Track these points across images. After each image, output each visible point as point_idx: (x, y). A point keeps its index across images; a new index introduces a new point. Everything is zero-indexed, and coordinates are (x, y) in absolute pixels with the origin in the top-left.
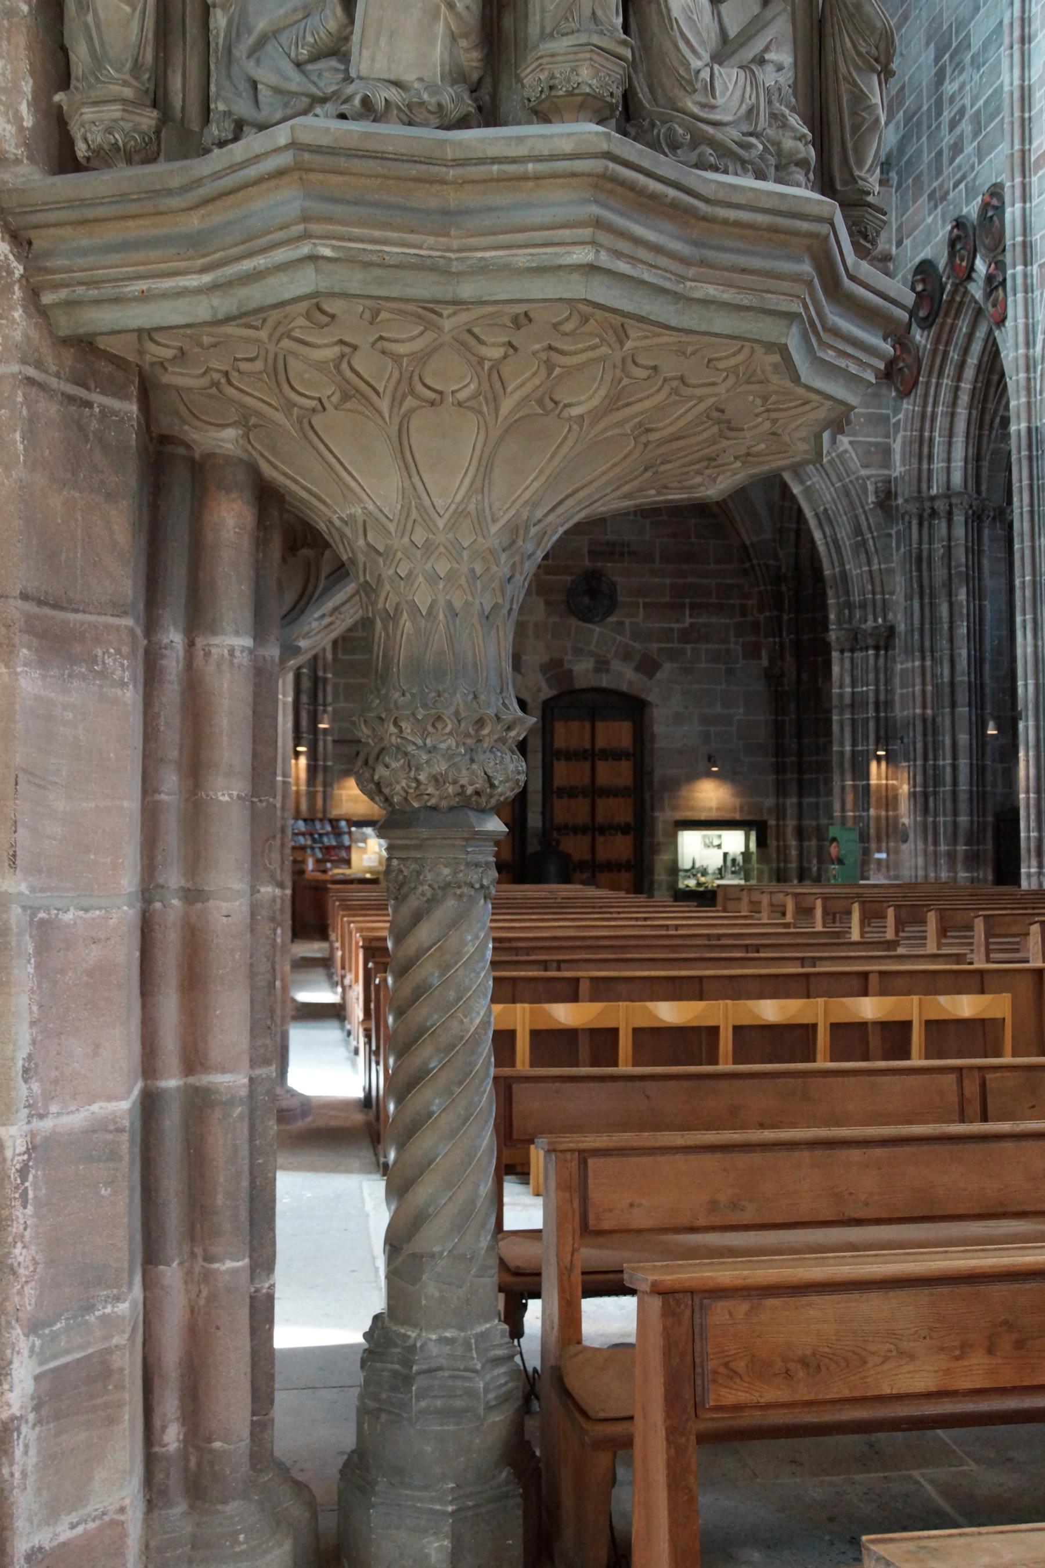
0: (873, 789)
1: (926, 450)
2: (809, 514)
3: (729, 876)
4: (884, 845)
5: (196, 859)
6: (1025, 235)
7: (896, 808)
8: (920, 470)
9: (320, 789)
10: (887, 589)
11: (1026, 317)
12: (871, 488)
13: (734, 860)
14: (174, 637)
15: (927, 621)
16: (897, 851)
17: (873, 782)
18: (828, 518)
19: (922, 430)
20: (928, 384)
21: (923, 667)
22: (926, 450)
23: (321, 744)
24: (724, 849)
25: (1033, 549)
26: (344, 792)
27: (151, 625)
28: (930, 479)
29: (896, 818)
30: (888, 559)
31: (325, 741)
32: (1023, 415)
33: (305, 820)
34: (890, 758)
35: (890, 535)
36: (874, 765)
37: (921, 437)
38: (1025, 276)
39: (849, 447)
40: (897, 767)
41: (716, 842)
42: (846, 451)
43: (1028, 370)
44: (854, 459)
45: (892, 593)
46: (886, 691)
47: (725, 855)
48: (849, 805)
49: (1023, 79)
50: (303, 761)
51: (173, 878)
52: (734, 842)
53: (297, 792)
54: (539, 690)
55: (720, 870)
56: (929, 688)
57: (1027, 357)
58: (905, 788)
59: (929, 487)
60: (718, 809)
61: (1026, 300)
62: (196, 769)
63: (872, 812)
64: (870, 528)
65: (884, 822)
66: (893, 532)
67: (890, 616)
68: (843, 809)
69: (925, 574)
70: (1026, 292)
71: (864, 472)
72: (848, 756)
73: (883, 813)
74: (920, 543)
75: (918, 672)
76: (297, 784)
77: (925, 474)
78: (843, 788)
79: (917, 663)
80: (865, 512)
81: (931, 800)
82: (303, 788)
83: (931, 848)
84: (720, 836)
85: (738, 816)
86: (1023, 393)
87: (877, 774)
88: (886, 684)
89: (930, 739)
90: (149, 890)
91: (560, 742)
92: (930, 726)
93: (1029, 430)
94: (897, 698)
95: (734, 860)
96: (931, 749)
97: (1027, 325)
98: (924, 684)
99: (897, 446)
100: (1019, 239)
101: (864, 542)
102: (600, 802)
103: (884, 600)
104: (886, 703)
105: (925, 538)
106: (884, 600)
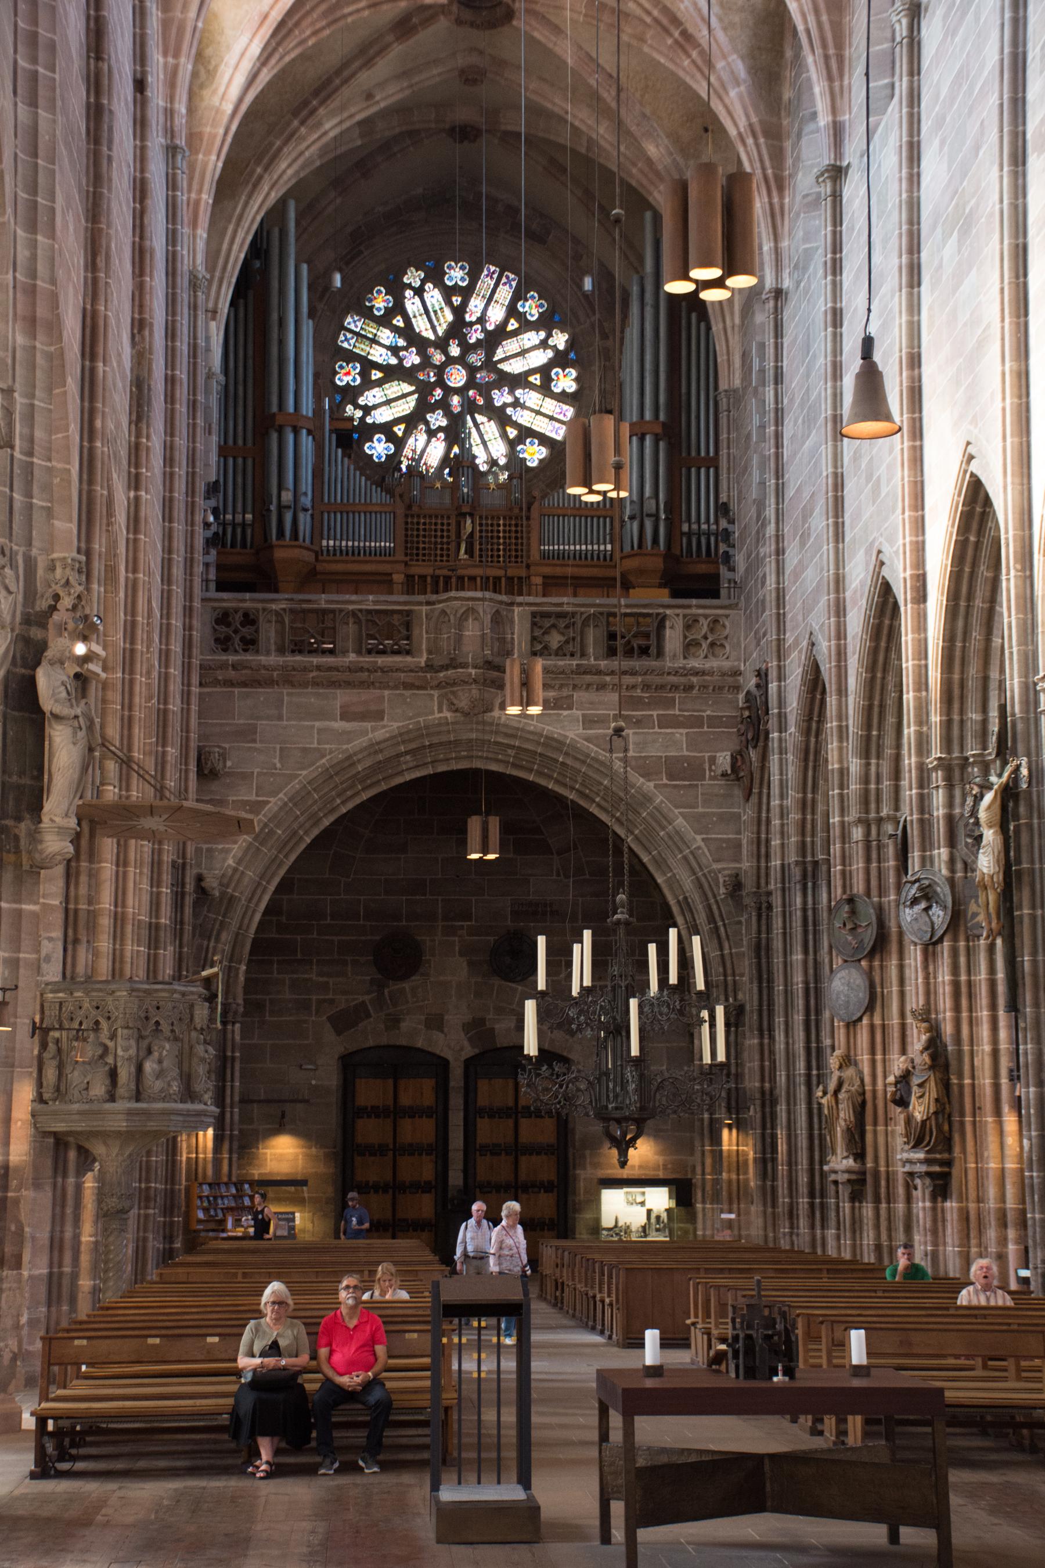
0: (725, 1154)
1: (763, 850)
2: (672, 902)
3: (654, 1233)
4: (735, 1206)
5: (62, 1225)
6: (780, 708)
7: (746, 1173)
8: (759, 868)
9: (226, 1156)
10: (737, 972)
11: (781, 774)
12: (721, 880)
13: (658, 1218)
14: (60, 1180)
15: (765, 1003)
16: (748, 1213)
17: (725, 1148)
18: (688, 904)
19: (759, 833)
20: (760, 794)
21: (761, 1045)
22: (763, 850)
23: (228, 1115)
24: (648, 1206)
25: (785, 963)
26: (268, 1151)
27: (55, 1177)
28: (767, 875)
29: (747, 1180)
30: (739, 944)
31: (232, 1113)
32: (779, 854)
33: (210, 1185)
34: (740, 1125)
35: (740, 923)
36: (725, 1133)
37: (759, 838)
38: (780, 740)
39: (702, 844)
40: (747, 1134)
41: (639, 1199)
42: (699, 848)
43: (782, 817)
44: (706, 856)
45: (742, 975)
46: (737, 1065)
47: (649, 1212)
48: (708, 1169)
49: (778, 583)
50: (210, 1132)
51: (58, 1229)
52: (659, 1199)
53: (205, 1159)
54: (462, 1049)
55: (644, 1228)
56: (767, 1063)
57: (781, 806)
58: (751, 1155)
59: (767, 883)
60: (640, 1167)
61: (781, 760)
62: (63, 1207)
63: (725, 1175)
64: (721, 915)
65: (735, 1184)
66: (743, 919)
67: (740, 996)
68: (703, 1174)
69: (764, 960)
70: (781, 753)
71: (716, 866)
72: (706, 1123)
73: (734, 1177)
74: (759, 932)
75: (757, 1049)
76: (205, 1153)
77: (763, 871)
78: (703, 1153)
79: (756, 1041)
80: (717, 902)
81: (769, 1166)
82: (210, 1155)
83: (770, 1210)
84: (643, 1193)
85: (661, 1175)
86: (778, 836)
87: (728, 1139)
88: (736, 1058)
89: (768, 1110)
90: (52, 1231)
91: (483, 1100)
92: (767, 1097)
93: (783, 865)
94: (746, 1071)
95: (658, 1218)
96: (768, 1121)
97: (781, 780)
98: (762, 1060)
99: (744, 842)
100: (776, 711)
101: (717, 928)
102: (523, 1160)
103: (734, 981)
104: (737, 1075)
105: (764, 928)
106: (734, 981)
